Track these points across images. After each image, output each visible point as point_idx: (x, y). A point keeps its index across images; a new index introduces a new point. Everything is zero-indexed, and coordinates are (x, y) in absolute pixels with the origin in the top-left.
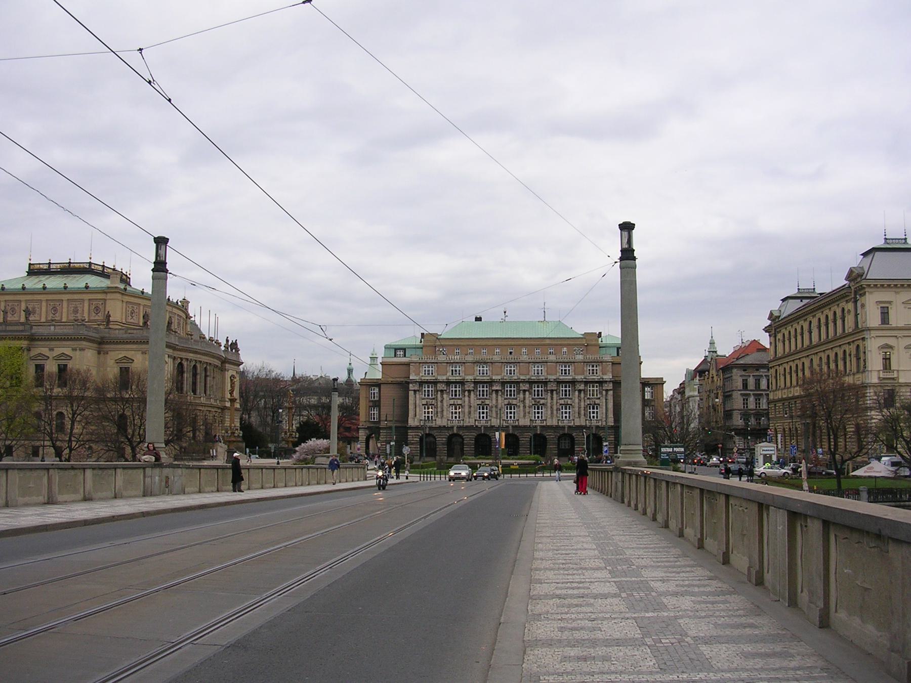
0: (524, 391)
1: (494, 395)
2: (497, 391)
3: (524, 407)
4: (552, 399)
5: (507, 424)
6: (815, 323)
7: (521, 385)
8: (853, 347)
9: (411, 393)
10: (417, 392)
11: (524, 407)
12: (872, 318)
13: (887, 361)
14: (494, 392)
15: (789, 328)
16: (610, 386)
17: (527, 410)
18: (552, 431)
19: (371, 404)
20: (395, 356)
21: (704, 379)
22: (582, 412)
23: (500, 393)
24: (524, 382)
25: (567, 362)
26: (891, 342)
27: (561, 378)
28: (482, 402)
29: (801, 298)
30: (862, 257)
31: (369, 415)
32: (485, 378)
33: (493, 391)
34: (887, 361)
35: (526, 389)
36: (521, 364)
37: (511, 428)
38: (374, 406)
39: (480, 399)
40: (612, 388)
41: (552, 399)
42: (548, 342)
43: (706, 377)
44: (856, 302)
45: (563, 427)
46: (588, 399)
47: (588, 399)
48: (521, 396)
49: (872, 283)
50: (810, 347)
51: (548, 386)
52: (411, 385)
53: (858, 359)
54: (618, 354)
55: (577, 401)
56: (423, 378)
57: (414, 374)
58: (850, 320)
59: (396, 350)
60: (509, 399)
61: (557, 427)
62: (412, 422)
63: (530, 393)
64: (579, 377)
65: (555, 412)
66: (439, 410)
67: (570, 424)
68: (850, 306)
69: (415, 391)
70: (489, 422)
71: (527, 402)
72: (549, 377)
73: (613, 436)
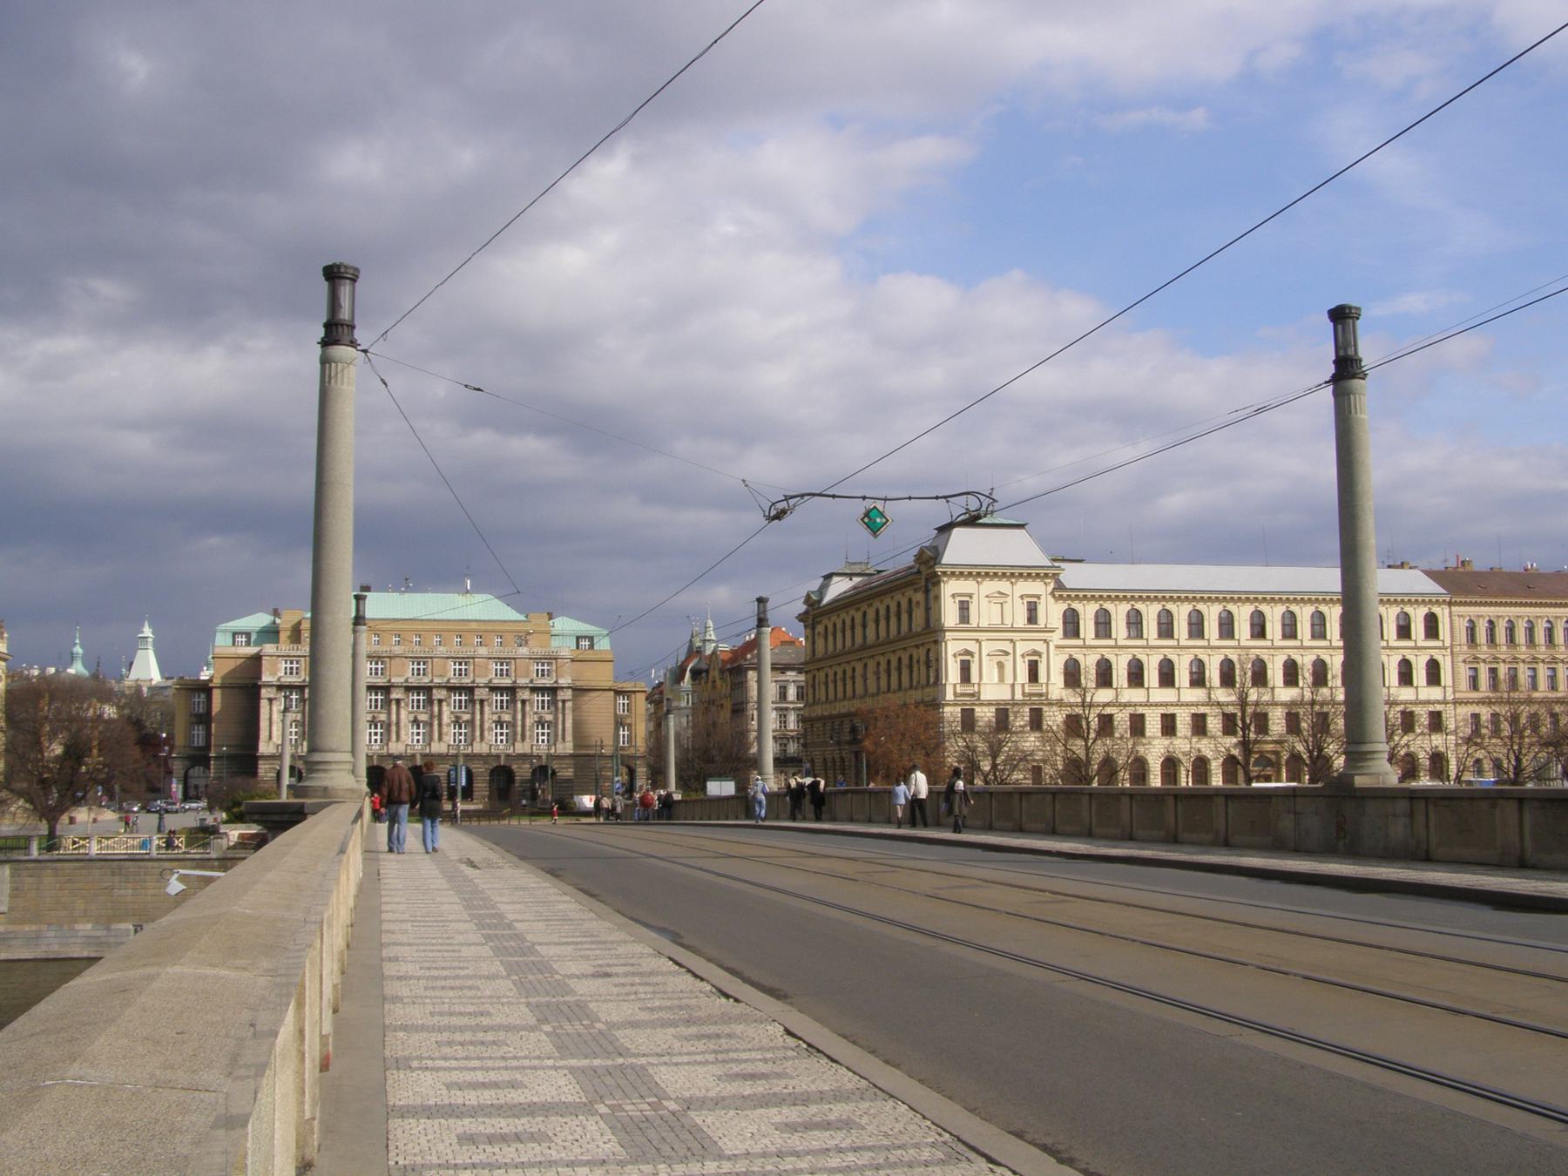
0: (440, 701)
1: (394, 707)
3: (440, 725)
5: (412, 752)
6: (871, 615)
7: (435, 691)
8: (922, 651)
9: (264, 704)
10: (274, 702)
11: (440, 725)
12: (950, 616)
14: (394, 702)
15: (834, 618)
16: (568, 694)
17: (445, 729)
18: (481, 762)
19: (194, 720)
20: (234, 644)
21: (700, 684)
22: (528, 733)
23: (403, 704)
24: (439, 687)
25: (505, 658)
27: (495, 681)
28: (374, 717)
29: (851, 576)
30: (936, 532)
31: (190, 737)
32: (379, 680)
35: (442, 697)
36: (435, 660)
37: (418, 757)
38: (198, 723)
39: (371, 713)
40: (570, 698)
42: (474, 626)
43: (703, 681)
44: (927, 591)
45: (498, 756)
46: (536, 713)
47: (536, 713)
49: (949, 570)
50: (864, 647)
51: (476, 693)
52: (263, 691)
53: (928, 667)
54: (578, 647)
56: (282, 680)
57: (268, 673)
58: (919, 614)
59: (235, 634)
60: (417, 712)
61: (489, 755)
62: (264, 748)
63: (449, 705)
64: (522, 681)
65: (486, 733)
67: (508, 752)
68: (919, 597)
69: (270, 700)
70: (385, 748)
72: (478, 680)
73: (572, 770)
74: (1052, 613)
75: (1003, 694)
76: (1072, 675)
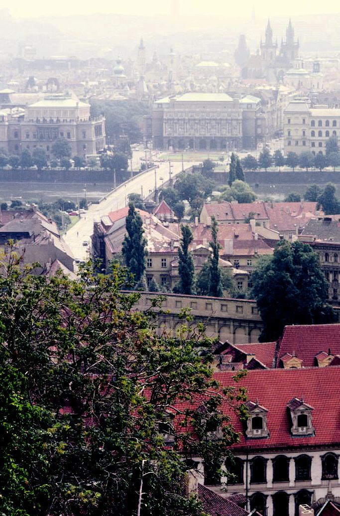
1: (196, 125)
2: (197, 123)
4: (218, 126)
9: (164, 124)
13: (289, 133)
16: (241, 121)
24: (207, 119)
26: (290, 128)
33: (195, 123)
34: (289, 133)
41: (218, 126)
48: (206, 125)
55: (228, 127)
62: (165, 135)
66: (175, 130)
69: (165, 123)
71: (209, 128)
74: (309, 121)
75: (296, 138)
76: (313, 134)
